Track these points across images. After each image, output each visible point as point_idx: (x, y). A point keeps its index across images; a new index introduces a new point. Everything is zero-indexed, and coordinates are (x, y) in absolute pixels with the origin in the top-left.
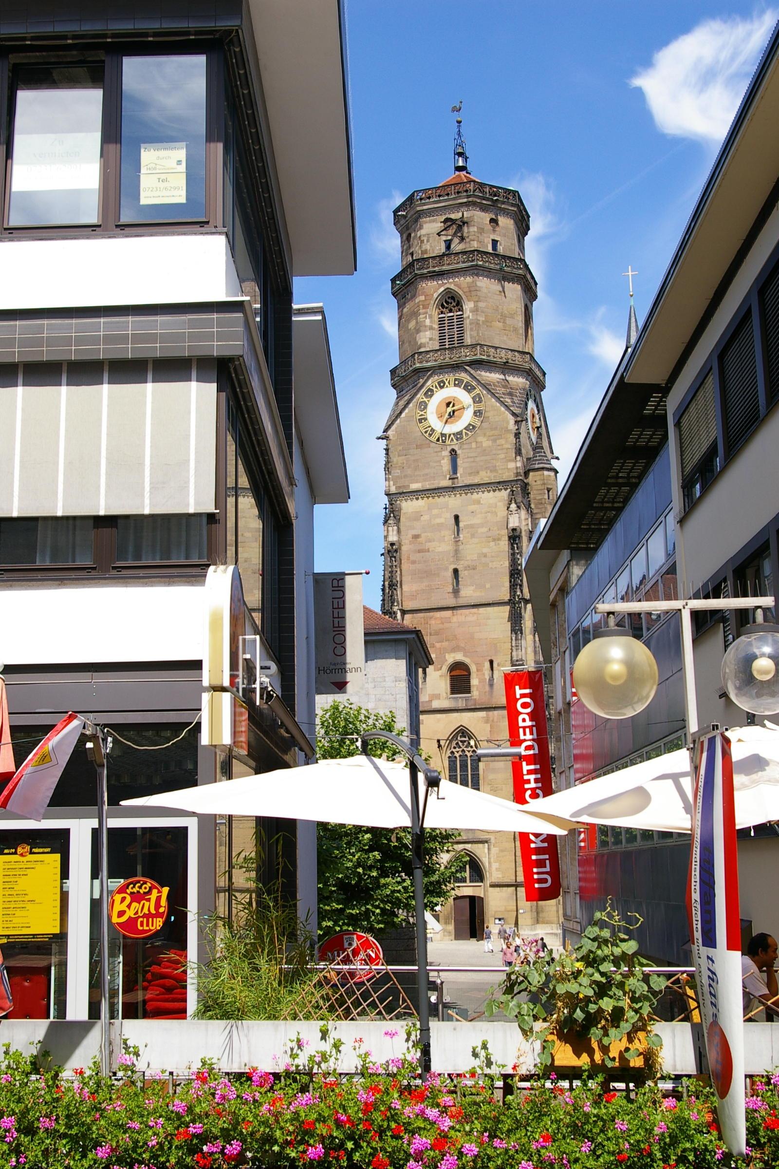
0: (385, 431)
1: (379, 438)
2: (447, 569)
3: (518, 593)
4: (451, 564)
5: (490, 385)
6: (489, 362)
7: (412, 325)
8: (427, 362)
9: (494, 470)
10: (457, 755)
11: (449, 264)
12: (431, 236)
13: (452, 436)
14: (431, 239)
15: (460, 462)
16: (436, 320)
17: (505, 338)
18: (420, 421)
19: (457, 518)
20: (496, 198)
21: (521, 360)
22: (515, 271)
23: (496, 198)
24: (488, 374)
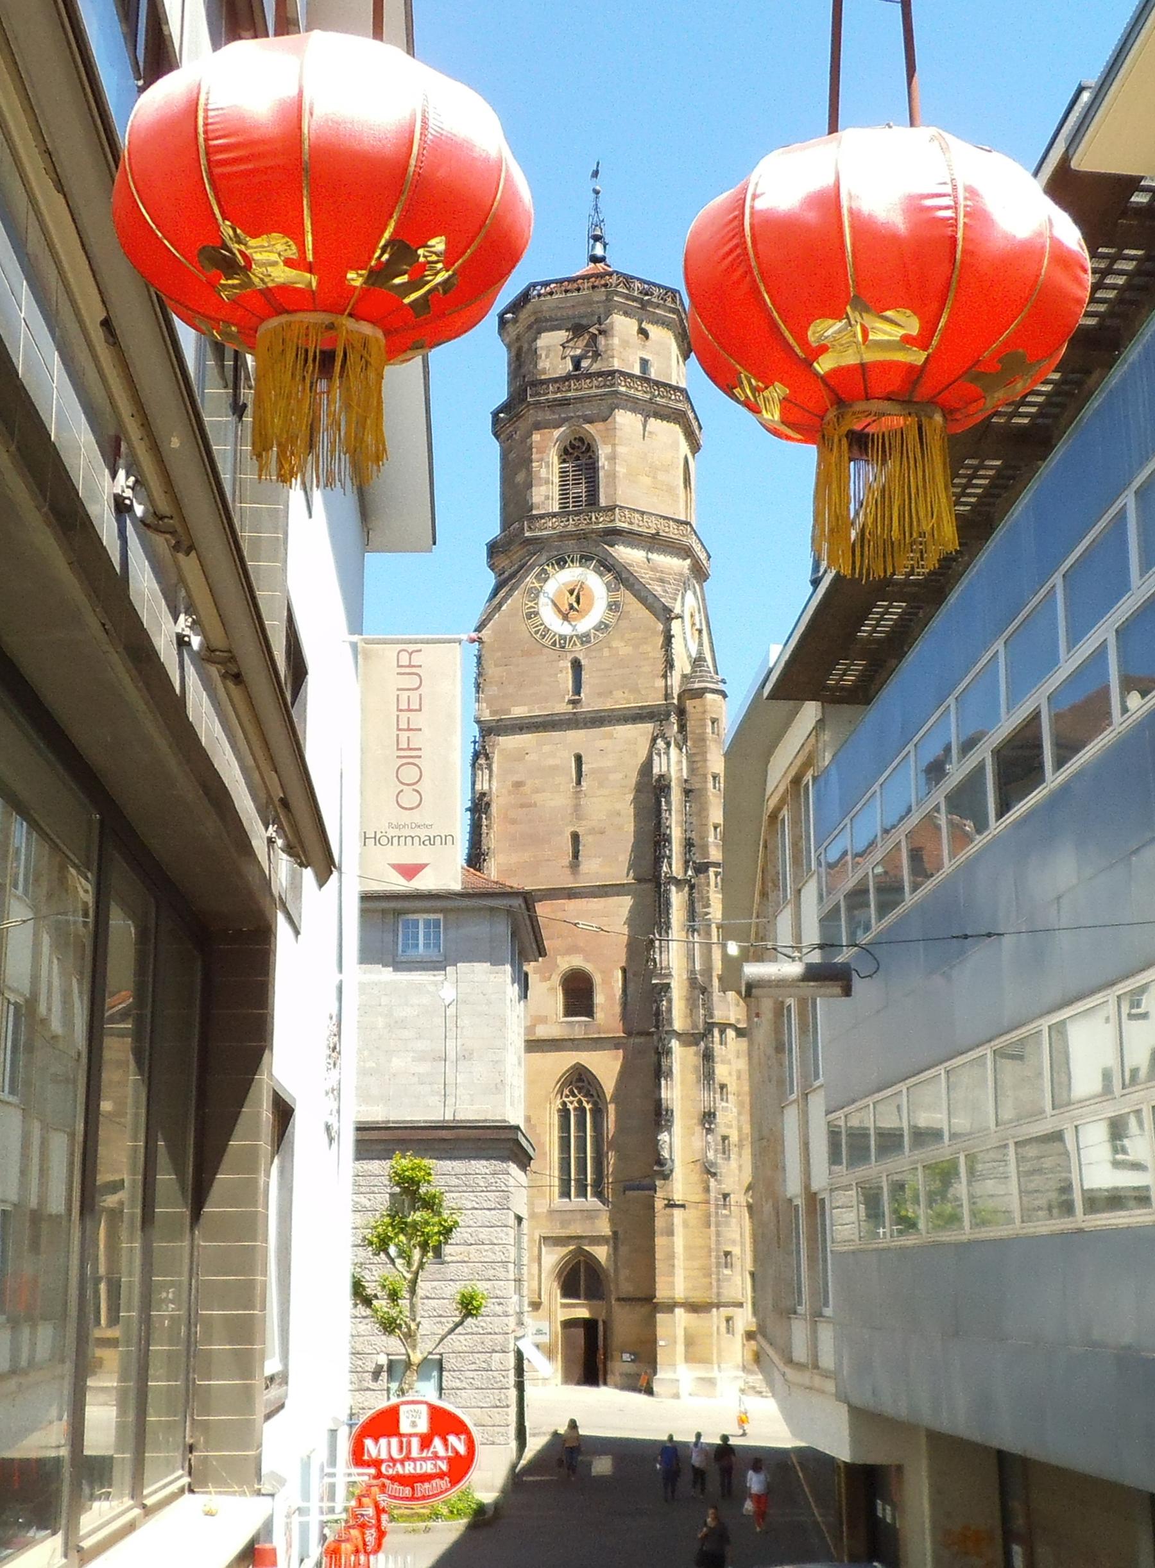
0: (479, 629)
3: (664, 869)
5: (631, 565)
6: (631, 533)
7: (520, 478)
8: (541, 530)
9: (635, 690)
10: (571, 1107)
11: (576, 390)
13: (575, 638)
14: (552, 355)
16: (556, 470)
18: (529, 616)
19: (579, 759)
21: (676, 532)
22: (672, 404)
23: (646, 298)
24: (629, 550)
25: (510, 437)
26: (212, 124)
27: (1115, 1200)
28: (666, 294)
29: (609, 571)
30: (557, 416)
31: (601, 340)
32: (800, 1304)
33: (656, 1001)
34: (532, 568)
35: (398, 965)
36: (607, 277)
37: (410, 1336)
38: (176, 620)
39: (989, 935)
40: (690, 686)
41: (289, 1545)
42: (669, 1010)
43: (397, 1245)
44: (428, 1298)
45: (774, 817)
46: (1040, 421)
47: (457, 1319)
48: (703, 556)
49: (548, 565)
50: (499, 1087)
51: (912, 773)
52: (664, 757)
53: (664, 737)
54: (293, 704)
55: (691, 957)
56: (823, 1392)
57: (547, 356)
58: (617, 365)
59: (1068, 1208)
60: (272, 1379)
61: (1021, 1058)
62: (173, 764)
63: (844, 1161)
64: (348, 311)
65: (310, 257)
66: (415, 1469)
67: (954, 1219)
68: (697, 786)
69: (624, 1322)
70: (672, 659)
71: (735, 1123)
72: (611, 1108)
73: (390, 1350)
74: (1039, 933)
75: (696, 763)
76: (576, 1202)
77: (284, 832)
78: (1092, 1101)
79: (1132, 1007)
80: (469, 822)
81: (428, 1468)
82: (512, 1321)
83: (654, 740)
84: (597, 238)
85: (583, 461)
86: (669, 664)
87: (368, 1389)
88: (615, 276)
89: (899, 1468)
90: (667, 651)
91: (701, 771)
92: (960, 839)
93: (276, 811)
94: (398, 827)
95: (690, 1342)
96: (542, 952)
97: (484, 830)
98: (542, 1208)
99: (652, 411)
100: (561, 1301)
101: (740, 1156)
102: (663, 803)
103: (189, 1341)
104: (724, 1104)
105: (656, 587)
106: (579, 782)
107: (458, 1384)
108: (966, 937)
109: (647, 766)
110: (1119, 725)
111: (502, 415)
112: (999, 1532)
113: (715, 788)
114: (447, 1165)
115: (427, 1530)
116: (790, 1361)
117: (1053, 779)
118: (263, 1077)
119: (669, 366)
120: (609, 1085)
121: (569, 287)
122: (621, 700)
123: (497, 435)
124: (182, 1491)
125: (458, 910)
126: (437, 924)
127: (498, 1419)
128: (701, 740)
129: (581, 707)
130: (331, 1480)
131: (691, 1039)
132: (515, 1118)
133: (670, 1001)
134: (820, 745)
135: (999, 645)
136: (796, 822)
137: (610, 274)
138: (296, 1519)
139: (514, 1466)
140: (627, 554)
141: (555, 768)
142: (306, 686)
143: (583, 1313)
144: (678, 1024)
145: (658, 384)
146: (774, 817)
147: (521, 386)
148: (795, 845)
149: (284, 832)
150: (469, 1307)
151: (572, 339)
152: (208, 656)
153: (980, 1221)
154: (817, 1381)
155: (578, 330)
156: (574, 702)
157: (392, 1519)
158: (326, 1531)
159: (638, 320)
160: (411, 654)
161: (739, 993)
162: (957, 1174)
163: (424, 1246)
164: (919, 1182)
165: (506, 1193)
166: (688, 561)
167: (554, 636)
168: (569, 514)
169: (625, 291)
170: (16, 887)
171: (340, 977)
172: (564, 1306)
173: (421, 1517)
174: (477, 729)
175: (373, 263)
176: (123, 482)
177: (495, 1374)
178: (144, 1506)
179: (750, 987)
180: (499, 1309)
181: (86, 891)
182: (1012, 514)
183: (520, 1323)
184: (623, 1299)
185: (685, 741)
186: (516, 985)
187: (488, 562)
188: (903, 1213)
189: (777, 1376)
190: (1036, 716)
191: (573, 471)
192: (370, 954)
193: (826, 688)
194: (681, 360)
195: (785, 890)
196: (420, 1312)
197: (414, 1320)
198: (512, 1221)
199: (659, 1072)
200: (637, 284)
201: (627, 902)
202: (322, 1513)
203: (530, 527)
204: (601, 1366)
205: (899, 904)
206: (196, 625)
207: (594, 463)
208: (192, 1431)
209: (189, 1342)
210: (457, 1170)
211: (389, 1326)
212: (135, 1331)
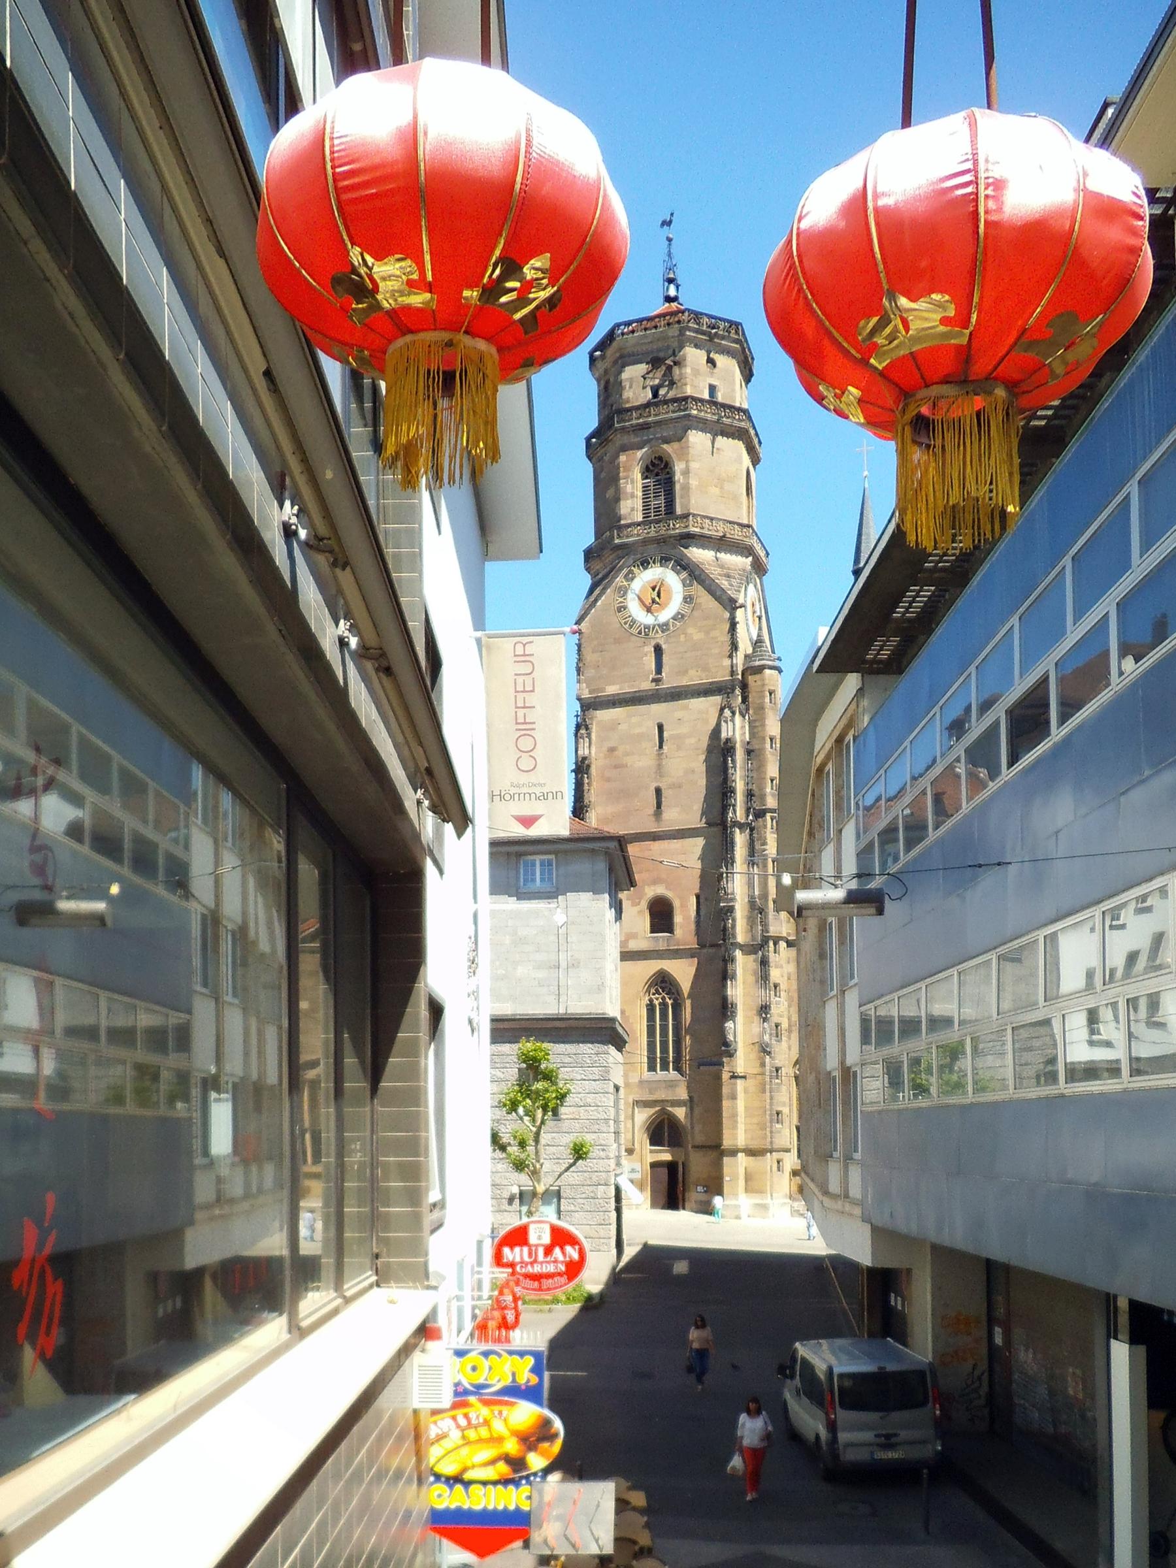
0: (578, 622)
3: (731, 815)
6: (702, 536)
7: (610, 493)
8: (628, 537)
9: (706, 669)
10: (656, 1002)
11: (656, 415)
16: (640, 486)
19: (661, 728)
21: (740, 534)
22: (736, 424)
23: (714, 331)
24: (701, 551)
25: (600, 459)
26: (338, 151)
27: (1091, 1071)
31: (676, 371)
32: (835, 1150)
33: (723, 920)
34: (621, 569)
35: (521, 896)
37: (535, 1174)
38: (337, 625)
39: (999, 864)
41: (450, 1323)
42: (734, 926)
43: (524, 1107)
44: (548, 1145)
45: (820, 770)
46: (1056, 422)
47: (572, 1161)
48: (762, 554)
50: (600, 988)
51: (938, 729)
53: (730, 708)
54: (432, 690)
55: (750, 885)
56: (851, 1215)
57: (631, 387)
58: (689, 391)
59: (1052, 1077)
60: (434, 1205)
61: (1019, 960)
62: (340, 743)
63: (873, 1041)
64: (464, 329)
65: (429, 277)
66: (542, 1268)
67: (959, 1086)
69: (697, 1164)
71: (786, 1013)
72: (688, 1003)
73: (521, 1183)
74: (1039, 862)
75: (756, 727)
76: (660, 1074)
77: (430, 795)
78: (1077, 995)
79: (1112, 920)
81: (551, 1268)
82: (612, 1163)
83: (722, 710)
84: (671, 281)
85: (662, 477)
86: (734, 646)
87: (506, 1211)
88: (686, 314)
89: (909, 1271)
91: (761, 734)
92: (976, 785)
93: (423, 778)
94: (518, 786)
95: (748, 1178)
96: (632, 883)
97: (586, 787)
98: (634, 1079)
99: (719, 430)
100: (649, 1147)
101: (789, 1038)
103: (372, 1179)
104: (777, 999)
106: (661, 747)
107: (573, 1208)
108: (980, 866)
109: (716, 731)
110: (1116, 684)
111: (594, 440)
112: (984, 1318)
113: (772, 747)
114: (561, 1048)
115: (550, 1311)
116: (826, 1193)
117: (1057, 733)
118: (420, 986)
119: (733, 390)
120: (686, 985)
121: (648, 326)
122: (695, 678)
123: (589, 457)
124: (371, 1286)
125: (566, 852)
126: (550, 864)
127: (602, 1233)
128: (761, 708)
130: (480, 1276)
131: (750, 949)
132: (613, 1011)
133: (734, 920)
134: (860, 709)
135: (1014, 620)
136: (838, 775)
137: (683, 312)
138: (455, 1304)
139: (614, 1268)
140: (699, 555)
141: (641, 737)
142: (441, 680)
143: (667, 1157)
144: (741, 936)
146: (820, 770)
148: (838, 793)
149: (430, 795)
150: (579, 1153)
151: (651, 371)
152: (364, 654)
153: (980, 1088)
154: (848, 1207)
155: (655, 363)
156: (655, 680)
157: (524, 1303)
158: (477, 1311)
160: (524, 645)
161: (791, 913)
162: (964, 1053)
163: (545, 1108)
164: (934, 1059)
165: (606, 1069)
166: (750, 558)
170: (226, 839)
171: (475, 907)
172: (651, 1151)
173: (546, 1302)
175: (485, 281)
176: (289, 511)
177: (601, 1201)
178: (345, 1297)
179: (800, 909)
180: (602, 1154)
181: (279, 842)
182: (1029, 505)
183: (618, 1164)
184: (697, 1147)
185: (747, 710)
186: (613, 910)
188: (918, 1081)
189: (816, 1203)
190: (1045, 680)
192: (497, 888)
193: (865, 661)
194: (743, 384)
195: (829, 830)
196: (543, 1155)
197: (538, 1161)
198: (612, 1089)
199: (725, 976)
200: (706, 319)
201: (700, 842)
202: (473, 1299)
204: (680, 1196)
205: (924, 839)
206: (353, 629)
208: (377, 1243)
209: (373, 1180)
210: (569, 1051)
211: (519, 1166)
212: (333, 1172)
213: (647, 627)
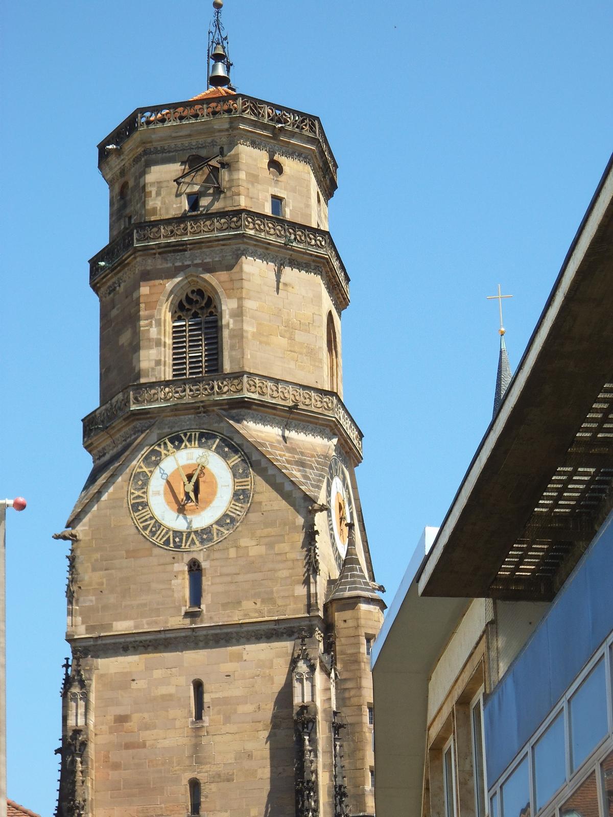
0: (71, 524)
1: (57, 537)
2: (178, 779)
4: (184, 771)
5: (263, 445)
6: (263, 405)
7: (125, 338)
8: (150, 402)
9: (269, 599)
11: (194, 233)
12: (164, 184)
13: (193, 535)
14: (163, 192)
15: (206, 582)
17: (292, 365)
18: (135, 507)
19: (198, 687)
20: (280, 125)
21: (319, 404)
22: (313, 250)
23: (280, 125)
24: (260, 427)
25: (112, 290)
28: (302, 121)
29: (236, 451)
30: (170, 265)
31: (225, 175)
34: (140, 447)
36: (231, 102)
40: (340, 595)
48: (353, 434)
49: (159, 445)
52: (307, 684)
53: (307, 659)
58: (243, 202)
68: (349, 720)
70: (317, 561)
80: (60, 767)
83: (294, 662)
84: (218, 58)
85: (202, 318)
86: (312, 567)
88: (240, 101)
90: (309, 550)
91: (354, 701)
97: (79, 777)
102: (307, 742)
105: (294, 472)
106: (199, 717)
109: (286, 694)
111: (102, 264)
119: (308, 206)
123: (95, 287)
128: (355, 660)
129: (202, 622)
137: (235, 98)
141: (167, 698)
145: (294, 225)
147: (125, 229)
151: (187, 174)
155: (195, 162)
159: (269, 152)
166: (335, 441)
167: (167, 533)
168: (185, 382)
169: (253, 118)
174: (70, 650)
185: (333, 663)
187: (84, 443)
191: (190, 331)
200: (267, 110)
203: (136, 399)
207: (216, 321)
213: (178, 533)
